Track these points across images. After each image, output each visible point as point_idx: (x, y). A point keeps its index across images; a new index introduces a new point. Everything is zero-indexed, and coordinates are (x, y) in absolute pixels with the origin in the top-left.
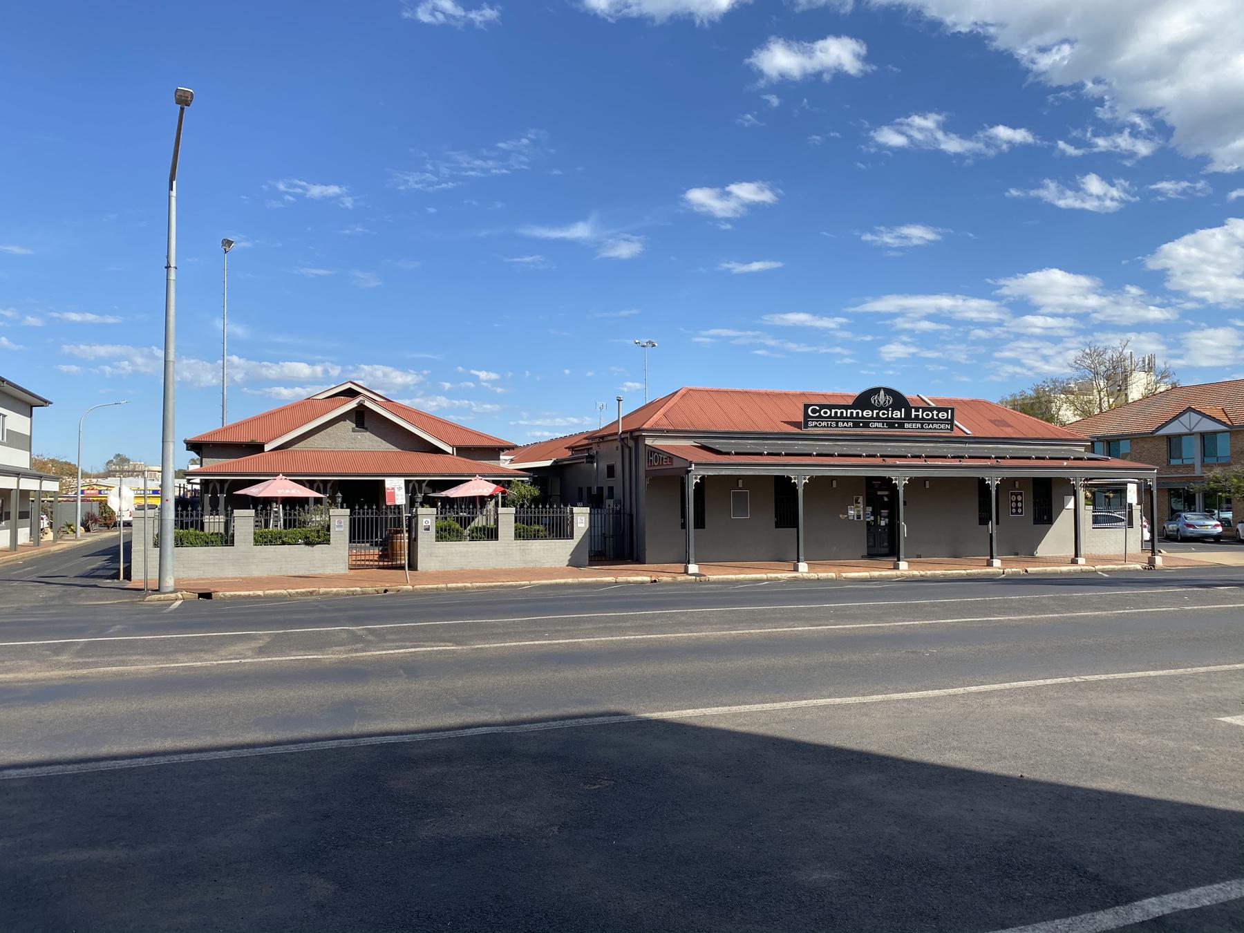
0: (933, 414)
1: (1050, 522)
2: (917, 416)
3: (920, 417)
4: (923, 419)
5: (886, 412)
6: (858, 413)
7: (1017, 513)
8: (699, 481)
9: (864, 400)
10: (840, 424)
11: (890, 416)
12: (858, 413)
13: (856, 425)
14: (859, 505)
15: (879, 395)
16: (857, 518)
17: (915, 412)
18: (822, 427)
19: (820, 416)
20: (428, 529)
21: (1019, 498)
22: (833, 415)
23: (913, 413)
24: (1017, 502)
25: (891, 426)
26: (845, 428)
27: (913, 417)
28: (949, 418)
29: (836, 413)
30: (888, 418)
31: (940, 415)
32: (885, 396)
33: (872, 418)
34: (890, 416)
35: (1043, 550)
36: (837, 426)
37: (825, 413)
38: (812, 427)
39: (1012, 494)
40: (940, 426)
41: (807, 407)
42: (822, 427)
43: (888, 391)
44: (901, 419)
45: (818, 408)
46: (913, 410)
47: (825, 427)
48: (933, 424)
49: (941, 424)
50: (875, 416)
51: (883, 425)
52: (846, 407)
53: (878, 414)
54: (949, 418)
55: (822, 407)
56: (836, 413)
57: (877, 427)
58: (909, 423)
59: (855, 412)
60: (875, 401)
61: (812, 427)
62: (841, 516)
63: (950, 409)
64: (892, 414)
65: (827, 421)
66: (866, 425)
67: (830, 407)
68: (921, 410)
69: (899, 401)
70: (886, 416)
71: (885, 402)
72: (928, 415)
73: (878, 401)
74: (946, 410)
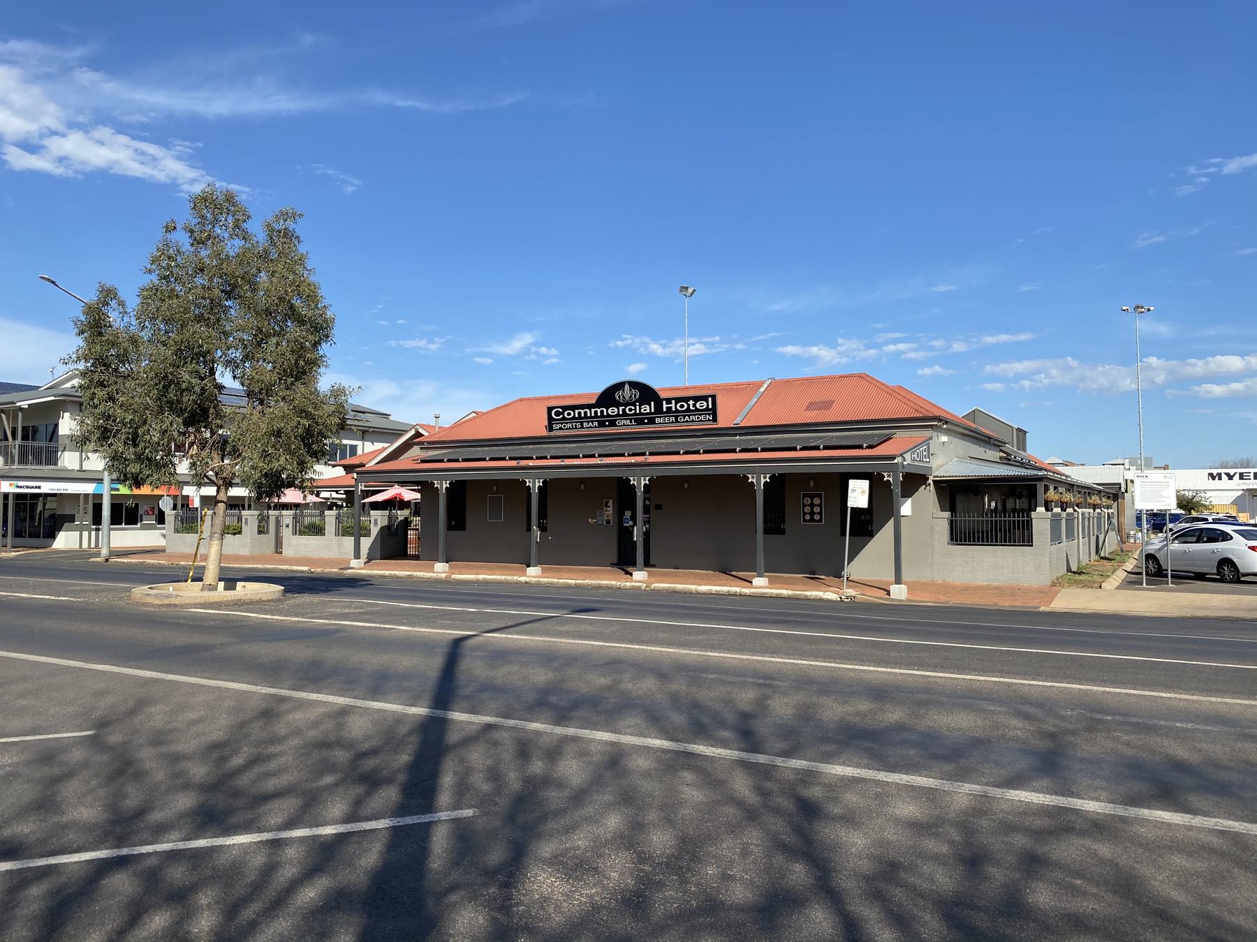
0: (689, 405)
1: (871, 535)
2: (669, 409)
3: (674, 409)
4: (677, 411)
5: (633, 408)
6: (602, 412)
7: (812, 520)
8: (885, 479)
9: (608, 397)
10: (585, 425)
11: (638, 412)
12: (602, 412)
13: (602, 424)
14: (608, 509)
15: (623, 390)
16: (607, 523)
17: (671, 407)
18: (567, 429)
19: (564, 418)
20: (288, 526)
21: (817, 501)
22: (577, 416)
23: (665, 406)
24: (812, 505)
25: (640, 422)
26: (591, 428)
27: (665, 410)
28: (710, 407)
29: (580, 413)
30: (635, 414)
31: (698, 405)
32: (631, 390)
33: (618, 415)
34: (638, 412)
35: (853, 569)
36: (582, 427)
37: (569, 414)
38: (557, 430)
39: (805, 496)
40: (698, 418)
41: (550, 409)
42: (567, 429)
43: (634, 385)
44: (651, 413)
45: (561, 410)
46: (664, 402)
47: (570, 428)
48: (689, 416)
49: (701, 415)
50: (621, 413)
51: (631, 422)
52: (590, 407)
53: (624, 410)
54: (710, 407)
55: (565, 408)
56: (580, 413)
57: (624, 425)
58: (660, 417)
59: (599, 410)
60: (619, 397)
61: (557, 430)
62: (590, 520)
63: (710, 396)
64: (640, 409)
65: (571, 423)
66: (613, 424)
67: (573, 408)
68: (673, 402)
69: (646, 393)
70: (633, 411)
71: (631, 396)
72: (682, 406)
73: (624, 397)
74: (705, 398)
